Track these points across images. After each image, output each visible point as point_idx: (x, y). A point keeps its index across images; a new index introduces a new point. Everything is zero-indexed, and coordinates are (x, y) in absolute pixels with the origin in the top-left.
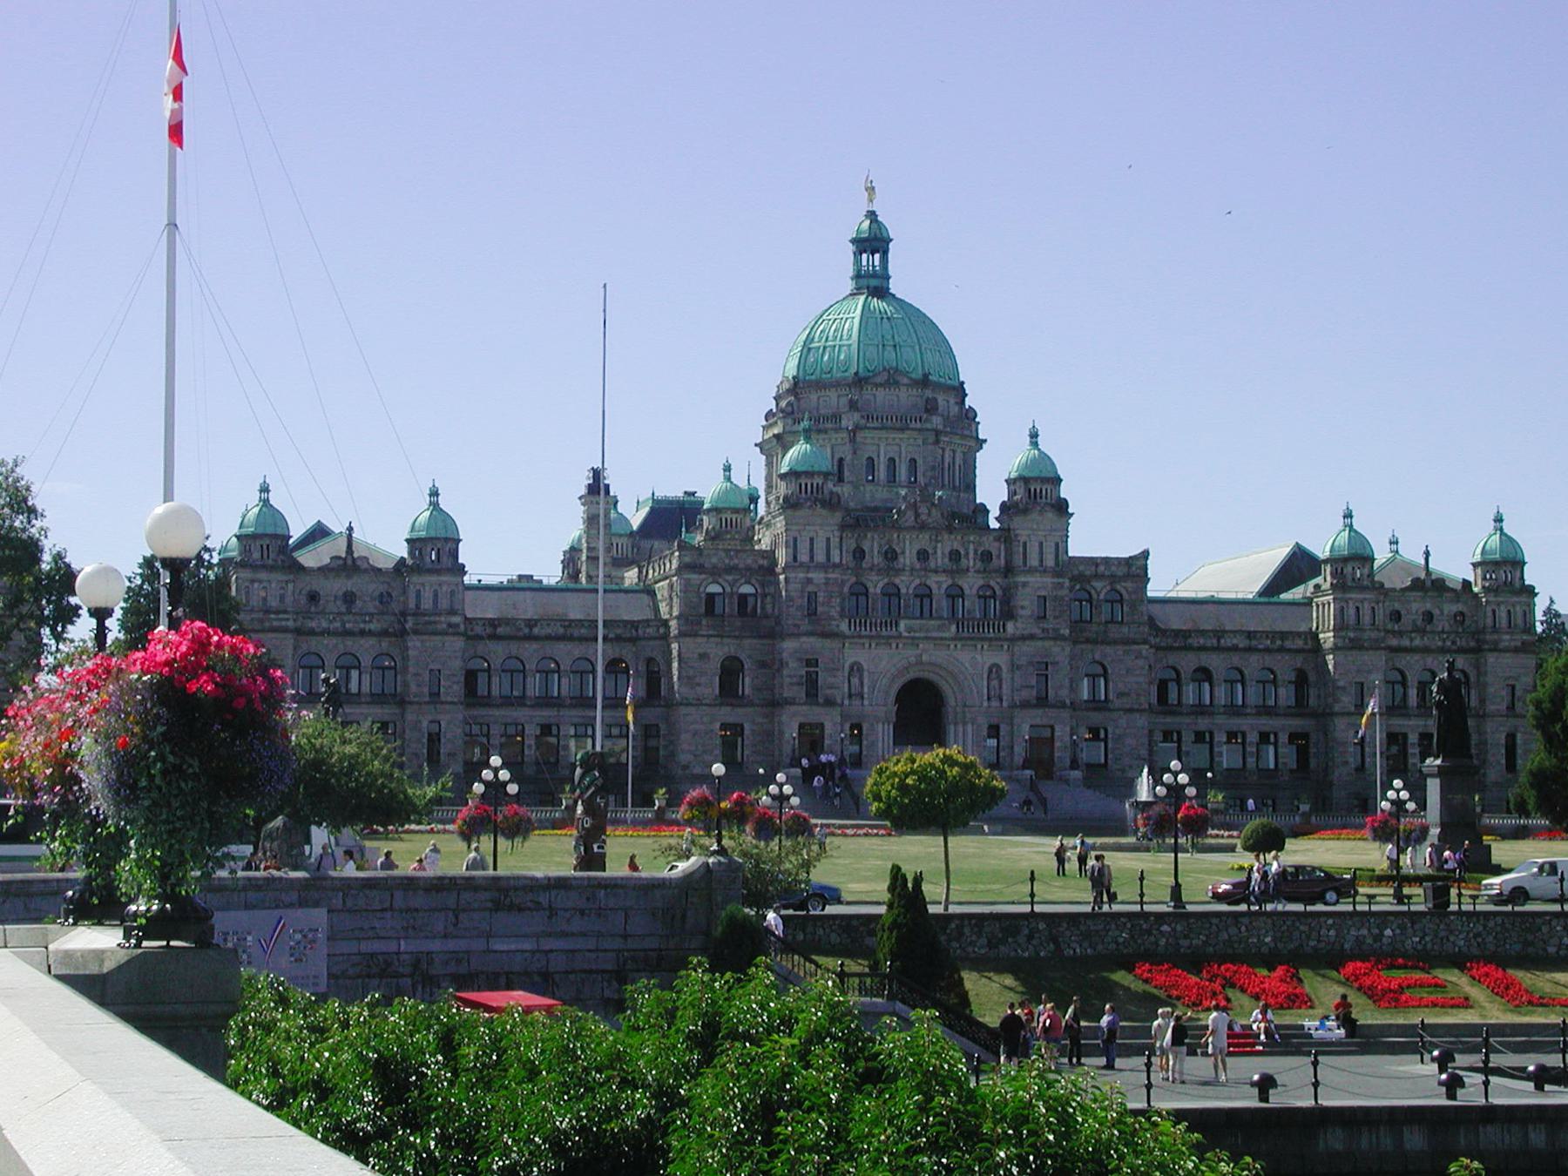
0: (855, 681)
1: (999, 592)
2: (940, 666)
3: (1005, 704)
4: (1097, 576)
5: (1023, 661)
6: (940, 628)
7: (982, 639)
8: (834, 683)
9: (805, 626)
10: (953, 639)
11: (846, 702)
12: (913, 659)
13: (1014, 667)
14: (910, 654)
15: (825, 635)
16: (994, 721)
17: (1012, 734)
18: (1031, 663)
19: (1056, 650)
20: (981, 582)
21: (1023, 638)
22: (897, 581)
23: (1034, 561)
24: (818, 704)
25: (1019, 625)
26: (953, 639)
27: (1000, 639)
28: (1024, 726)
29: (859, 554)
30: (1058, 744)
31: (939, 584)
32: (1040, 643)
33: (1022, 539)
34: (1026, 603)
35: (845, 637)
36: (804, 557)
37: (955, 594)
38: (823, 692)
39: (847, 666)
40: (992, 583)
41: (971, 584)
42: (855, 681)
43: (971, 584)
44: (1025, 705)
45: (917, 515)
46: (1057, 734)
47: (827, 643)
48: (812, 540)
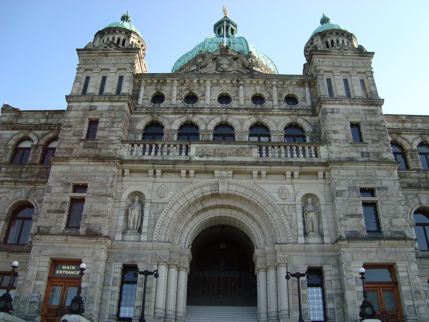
0: (135, 213)
1: (308, 129)
2: (242, 198)
3: (327, 240)
4: (409, 131)
5: (343, 186)
6: (238, 153)
7: (291, 164)
8: (106, 212)
9: (79, 149)
10: (256, 164)
11: (119, 237)
12: (207, 191)
13: (333, 195)
14: (203, 184)
15: (99, 159)
16: (316, 262)
17: (340, 277)
18: (352, 189)
19: (381, 173)
20: (288, 120)
21: (340, 162)
22: (195, 119)
23: (340, 90)
24: (78, 235)
25: (334, 148)
26: (256, 164)
27: (312, 164)
28: (356, 261)
29: (158, 98)
30: (404, 288)
31: (242, 123)
32: (361, 166)
33: (326, 76)
34: (338, 127)
35: (122, 161)
36: (92, 89)
37: (259, 130)
38: (89, 220)
39: (125, 196)
40: (300, 121)
41: (277, 123)
42: (135, 213)
43: (277, 123)
44: (353, 237)
45: (218, 65)
46: (401, 274)
47: (101, 167)
48: (104, 79)
